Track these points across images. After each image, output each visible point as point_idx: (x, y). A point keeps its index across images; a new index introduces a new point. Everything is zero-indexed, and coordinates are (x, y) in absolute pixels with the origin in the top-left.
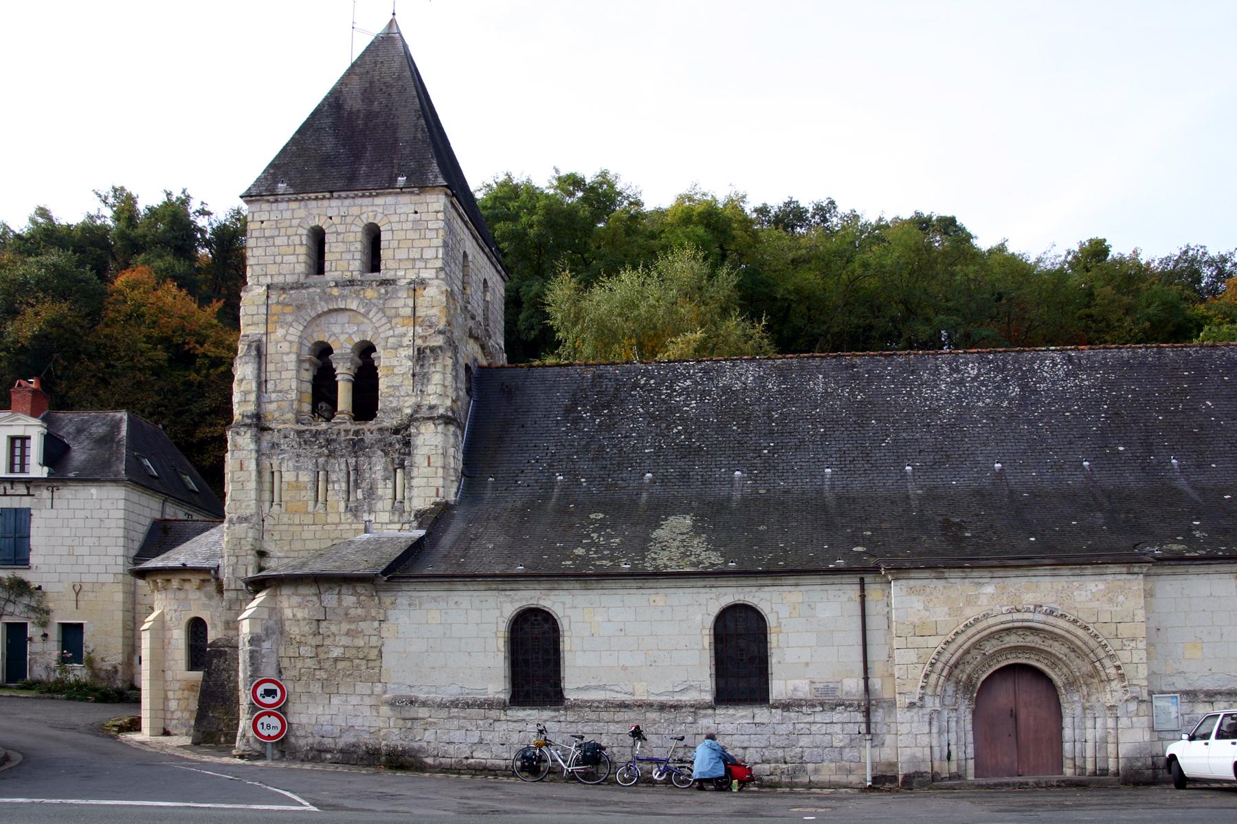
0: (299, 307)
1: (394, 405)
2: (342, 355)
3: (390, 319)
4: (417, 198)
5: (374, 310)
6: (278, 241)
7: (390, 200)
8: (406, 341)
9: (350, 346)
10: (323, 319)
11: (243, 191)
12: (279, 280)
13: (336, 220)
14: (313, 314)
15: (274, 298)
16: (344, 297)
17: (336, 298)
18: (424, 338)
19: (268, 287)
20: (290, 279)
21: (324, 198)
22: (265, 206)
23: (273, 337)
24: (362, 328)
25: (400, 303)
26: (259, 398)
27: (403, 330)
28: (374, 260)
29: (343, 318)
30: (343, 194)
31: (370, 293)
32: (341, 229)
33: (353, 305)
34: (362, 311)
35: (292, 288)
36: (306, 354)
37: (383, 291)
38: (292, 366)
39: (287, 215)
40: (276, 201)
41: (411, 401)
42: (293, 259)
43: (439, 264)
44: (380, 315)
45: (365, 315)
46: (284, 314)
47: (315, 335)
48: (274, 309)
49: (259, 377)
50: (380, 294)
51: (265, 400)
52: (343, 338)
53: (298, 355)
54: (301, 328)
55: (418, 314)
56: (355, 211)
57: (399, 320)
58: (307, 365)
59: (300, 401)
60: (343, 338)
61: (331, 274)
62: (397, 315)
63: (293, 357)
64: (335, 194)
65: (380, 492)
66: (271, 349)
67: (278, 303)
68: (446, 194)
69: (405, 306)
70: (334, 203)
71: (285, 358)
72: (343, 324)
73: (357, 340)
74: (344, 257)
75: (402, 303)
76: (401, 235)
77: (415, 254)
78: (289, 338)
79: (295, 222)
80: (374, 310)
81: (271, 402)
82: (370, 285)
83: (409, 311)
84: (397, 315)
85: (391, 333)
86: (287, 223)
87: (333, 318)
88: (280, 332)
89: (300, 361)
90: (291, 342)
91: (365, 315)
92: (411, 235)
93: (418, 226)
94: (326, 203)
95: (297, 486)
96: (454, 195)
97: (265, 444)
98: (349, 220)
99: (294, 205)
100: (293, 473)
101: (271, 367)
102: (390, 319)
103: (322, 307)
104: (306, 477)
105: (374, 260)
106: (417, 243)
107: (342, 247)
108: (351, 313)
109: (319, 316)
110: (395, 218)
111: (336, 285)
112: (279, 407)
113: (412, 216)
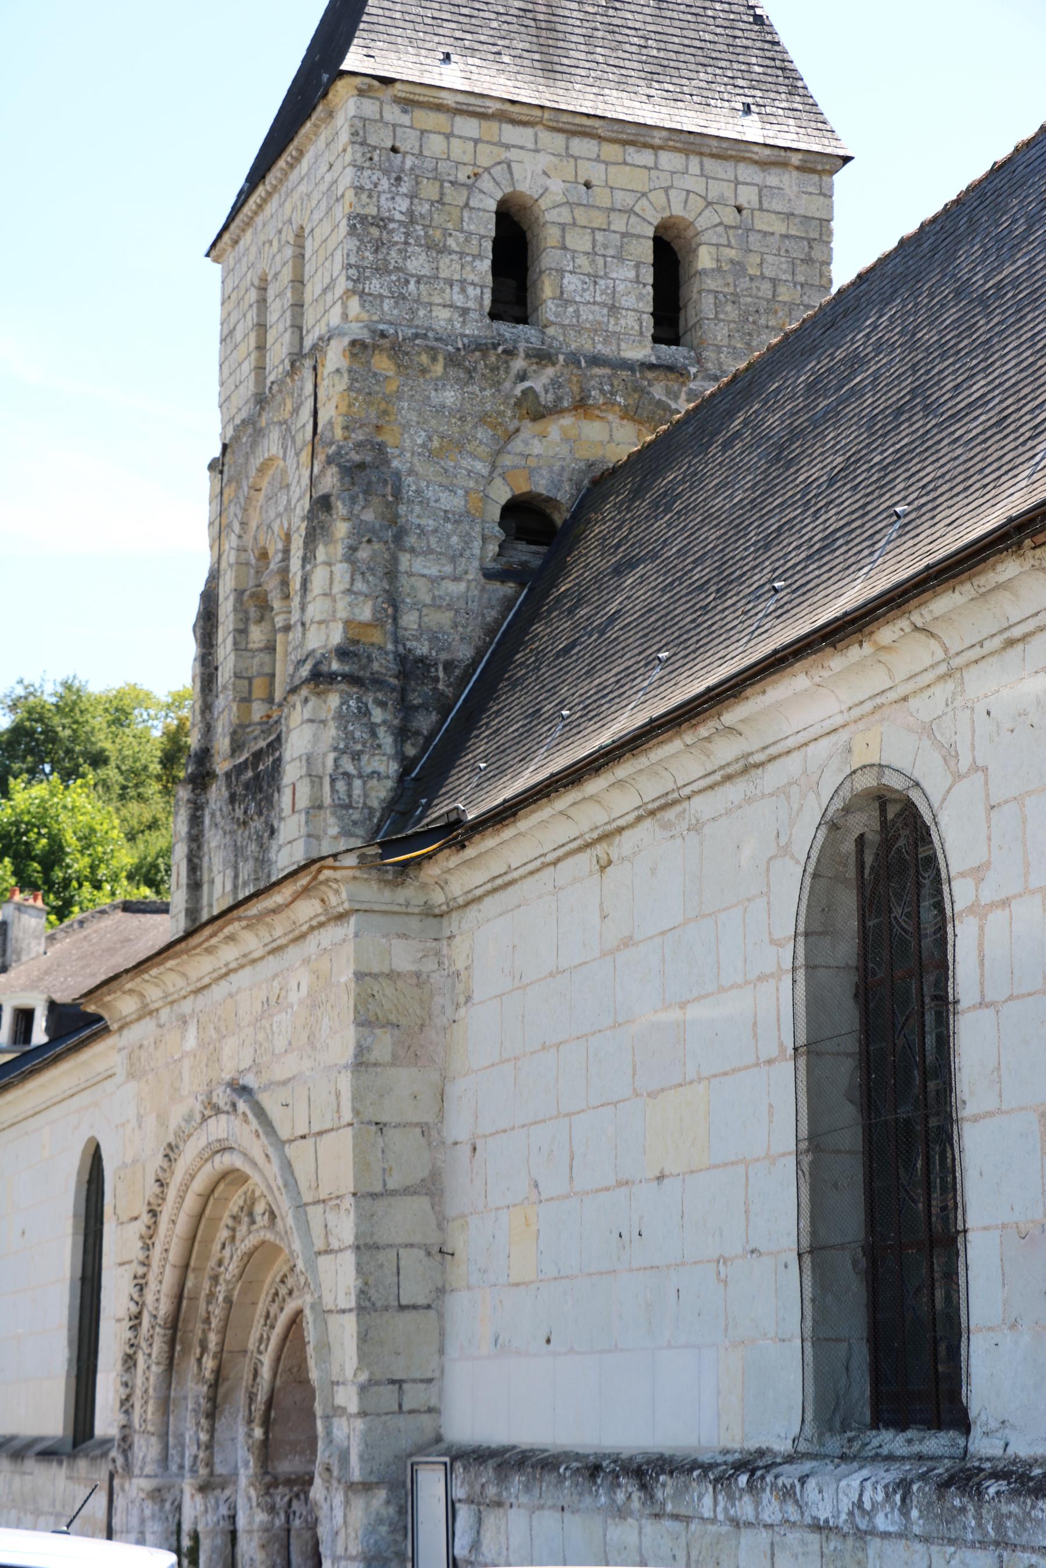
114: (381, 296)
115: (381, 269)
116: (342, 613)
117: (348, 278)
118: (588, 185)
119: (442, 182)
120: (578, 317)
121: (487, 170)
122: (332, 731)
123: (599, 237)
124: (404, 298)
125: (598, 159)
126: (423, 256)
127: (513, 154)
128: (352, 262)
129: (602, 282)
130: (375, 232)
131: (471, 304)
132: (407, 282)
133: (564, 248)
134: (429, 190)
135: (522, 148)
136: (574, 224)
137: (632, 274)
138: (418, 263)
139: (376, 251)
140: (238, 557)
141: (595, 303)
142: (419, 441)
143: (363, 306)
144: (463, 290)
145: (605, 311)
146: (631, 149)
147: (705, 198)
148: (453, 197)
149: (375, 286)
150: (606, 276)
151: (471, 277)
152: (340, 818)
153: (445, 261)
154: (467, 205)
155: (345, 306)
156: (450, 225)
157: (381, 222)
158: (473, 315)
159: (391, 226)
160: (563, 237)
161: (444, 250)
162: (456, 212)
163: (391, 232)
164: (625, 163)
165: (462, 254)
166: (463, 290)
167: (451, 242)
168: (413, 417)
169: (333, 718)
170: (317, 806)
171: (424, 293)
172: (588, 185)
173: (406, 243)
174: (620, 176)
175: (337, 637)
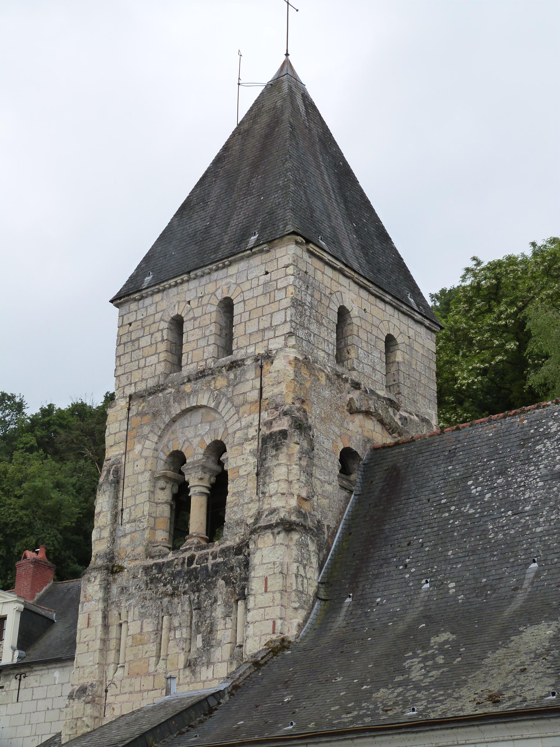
0: (155, 415)
1: (238, 516)
2: (193, 463)
3: (237, 408)
4: (265, 257)
5: (224, 401)
6: (144, 342)
7: (242, 265)
8: (252, 432)
9: (201, 451)
10: (177, 425)
11: (111, 298)
13: (194, 304)
14: (167, 419)
15: (134, 409)
16: (195, 392)
17: (189, 395)
18: (269, 424)
20: (151, 383)
21: (183, 282)
22: (133, 306)
23: (131, 455)
24: (215, 425)
27: (249, 419)
28: (227, 342)
29: (197, 417)
30: (199, 272)
31: (221, 382)
32: (198, 312)
33: (204, 399)
34: (212, 405)
35: (150, 394)
36: (161, 468)
37: (232, 376)
38: (146, 487)
39: (152, 310)
40: (142, 298)
43: (287, 328)
44: (229, 405)
45: (215, 410)
46: (141, 426)
47: (170, 444)
48: (135, 421)
49: (116, 507)
50: (229, 381)
51: (120, 534)
52: (196, 441)
53: (153, 473)
54: (156, 439)
55: (264, 396)
56: (211, 288)
57: (246, 407)
58: (162, 483)
59: (153, 529)
60: (193, 441)
61: (188, 369)
62: (245, 402)
63: (147, 475)
64: (192, 275)
67: (138, 414)
68: (297, 243)
69: (253, 388)
70: (193, 284)
71: (141, 479)
72: (196, 426)
73: (208, 441)
74: (200, 348)
75: (249, 386)
76: (251, 304)
77: (265, 324)
78: (145, 454)
79: (158, 317)
80: (224, 401)
81: (125, 536)
82: (220, 372)
83: (255, 394)
84: (245, 402)
85: (238, 425)
86: (151, 319)
87: (186, 421)
90: (146, 458)
91: (215, 410)
92: (262, 301)
93: (269, 290)
94: (185, 286)
95: (138, 641)
96: (308, 242)
97: (115, 589)
98: (205, 300)
100: (135, 623)
101: (127, 492)
102: (237, 408)
103: (176, 409)
104: (149, 627)
105: (227, 342)
106: (268, 310)
107: (198, 333)
108: (203, 410)
109: (174, 420)
111: (189, 381)
112: (132, 540)
113: (263, 279)
114: (302, 338)
115: (302, 326)
116: (296, 492)
117: (292, 327)
118: (365, 310)
119: (321, 293)
120: (364, 369)
121: (335, 292)
122: (295, 552)
123: (369, 335)
124: (310, 342)
125: (367, 301)
126: (315, 325)
127: (342, 289)
128: (294, 319)
129: (370, 356)
130: (300, 307)
131: (330, 352)
132: (310, 335)
133: (358, 336)
134: (317, 295)
135: (345, 287)
136: (361, 327)
137: (379, 356)
138: (314, 327)
139: (300, 318)
140: (153, 453)
141: (368, 365)
142: (318, 412)
143: (296, 342)
144: (328, 346)
145: (371, 369)
146: (378, 300)
147: (399, 329)
148: (325, 301)
149: (301, 333)
150: (371, 354)
151: (330, 340)
152: (300, 599)
153: (323, 329)
154: (329, 306)
155: (286, 339)
156: (323, 314)
157: (302, 304)
158: (331, 357)
159: (306, 307)
160: (358, 331)
161: (322, 324)
162: (325, 308)
163: (305, 310)
164: (376, 305)
165: (328, 329)
166: (328, 346)
167: (324, 321)
168: (315, 399)
169: (296, 545)
170: (283, 591)
171: (316, 342)
172: (365, 310)
173: (310, 317)
174: (376, 311)
175: (293, 502)
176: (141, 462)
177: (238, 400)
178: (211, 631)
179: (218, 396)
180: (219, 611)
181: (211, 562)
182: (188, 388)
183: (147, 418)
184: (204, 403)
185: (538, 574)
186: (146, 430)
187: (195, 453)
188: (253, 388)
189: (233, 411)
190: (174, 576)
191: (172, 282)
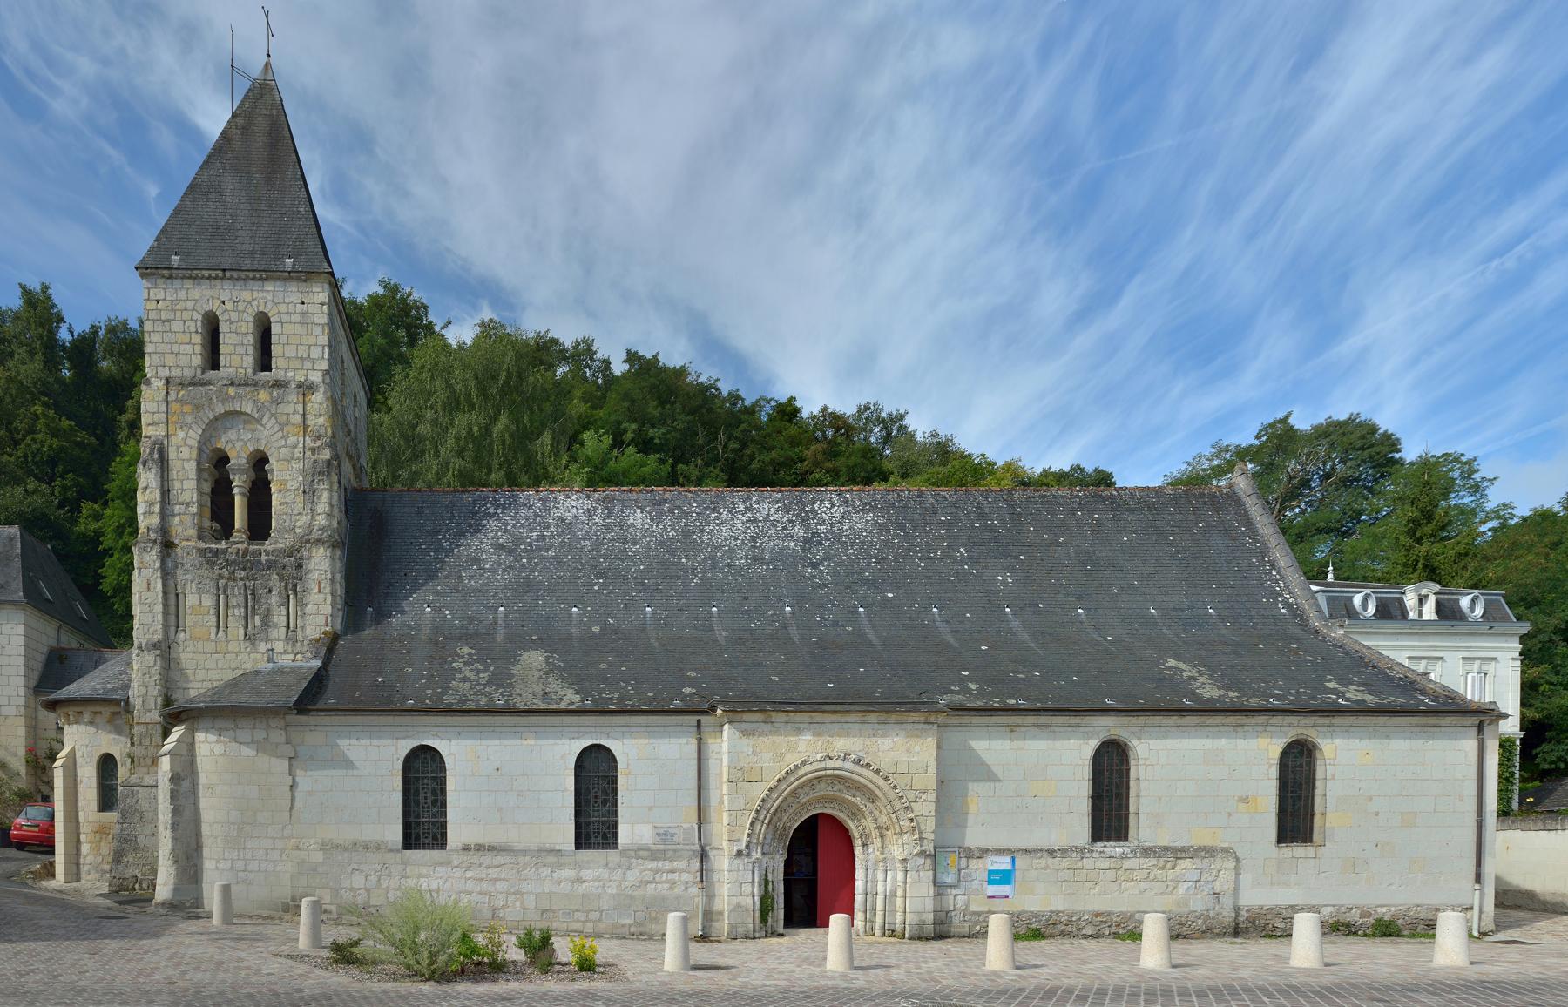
0: (198, 407)
6: (176, 326)
8: (297, 453)
12: (176, 373)
13: (229, 305)
19: (168, 381)
20: (188, 373)
21: (216, 278)
25: (290, 409)
26: (162, 509)
28: (264, 359)
31: (263, 395)
32: (234, 316)
33: (248, 408)
38: (193, 475)
40: (171, 277)
41: (303, 520)
42: (188, 349)
44: (273, 421)
46: (183, 414)
48: (174, 407)
53: (199, 463)
56: (246, 295)
61: (225, 371)
63: (193, 465)
65: (275, 619)
66: (172, 454)
67: (177, 400)
69: (296, 412)
70: (227, 285)
71: (186, 465)
74: (237, 352)
76: (289, 329)
77: (303, 353)
79: (190, 304)
83: (297, 419)
86: (181, 306)
88: (181, 434)
89: (199, 470)
92: (300, 329)
98: (241, 306)
99: (188, 284)
103: (220, 409)
104: (208, 601)
105: (264, 359)
110: (283, 308)
111: (232, 384)
176: (186, 450)
177: (283, 419)
178: (268, 613)
179: (260, 407)
180: (274, 600)
181: (264, 558)
182: (231, 391)
183: (187, 409)
184: (248, 411)
185: (506, 615)
186: (189, 419)
187: (239, 456)
188: (296, 412)
189: (277, 428)
190: (229, 563)
191: (206, 273)
